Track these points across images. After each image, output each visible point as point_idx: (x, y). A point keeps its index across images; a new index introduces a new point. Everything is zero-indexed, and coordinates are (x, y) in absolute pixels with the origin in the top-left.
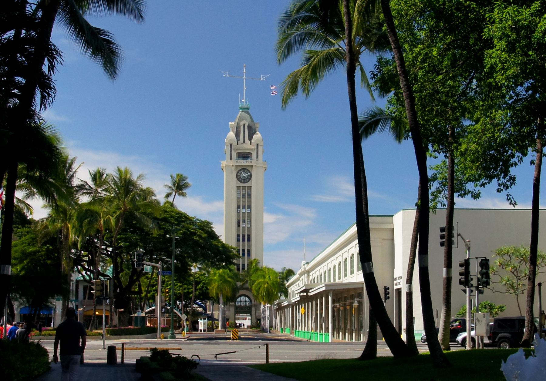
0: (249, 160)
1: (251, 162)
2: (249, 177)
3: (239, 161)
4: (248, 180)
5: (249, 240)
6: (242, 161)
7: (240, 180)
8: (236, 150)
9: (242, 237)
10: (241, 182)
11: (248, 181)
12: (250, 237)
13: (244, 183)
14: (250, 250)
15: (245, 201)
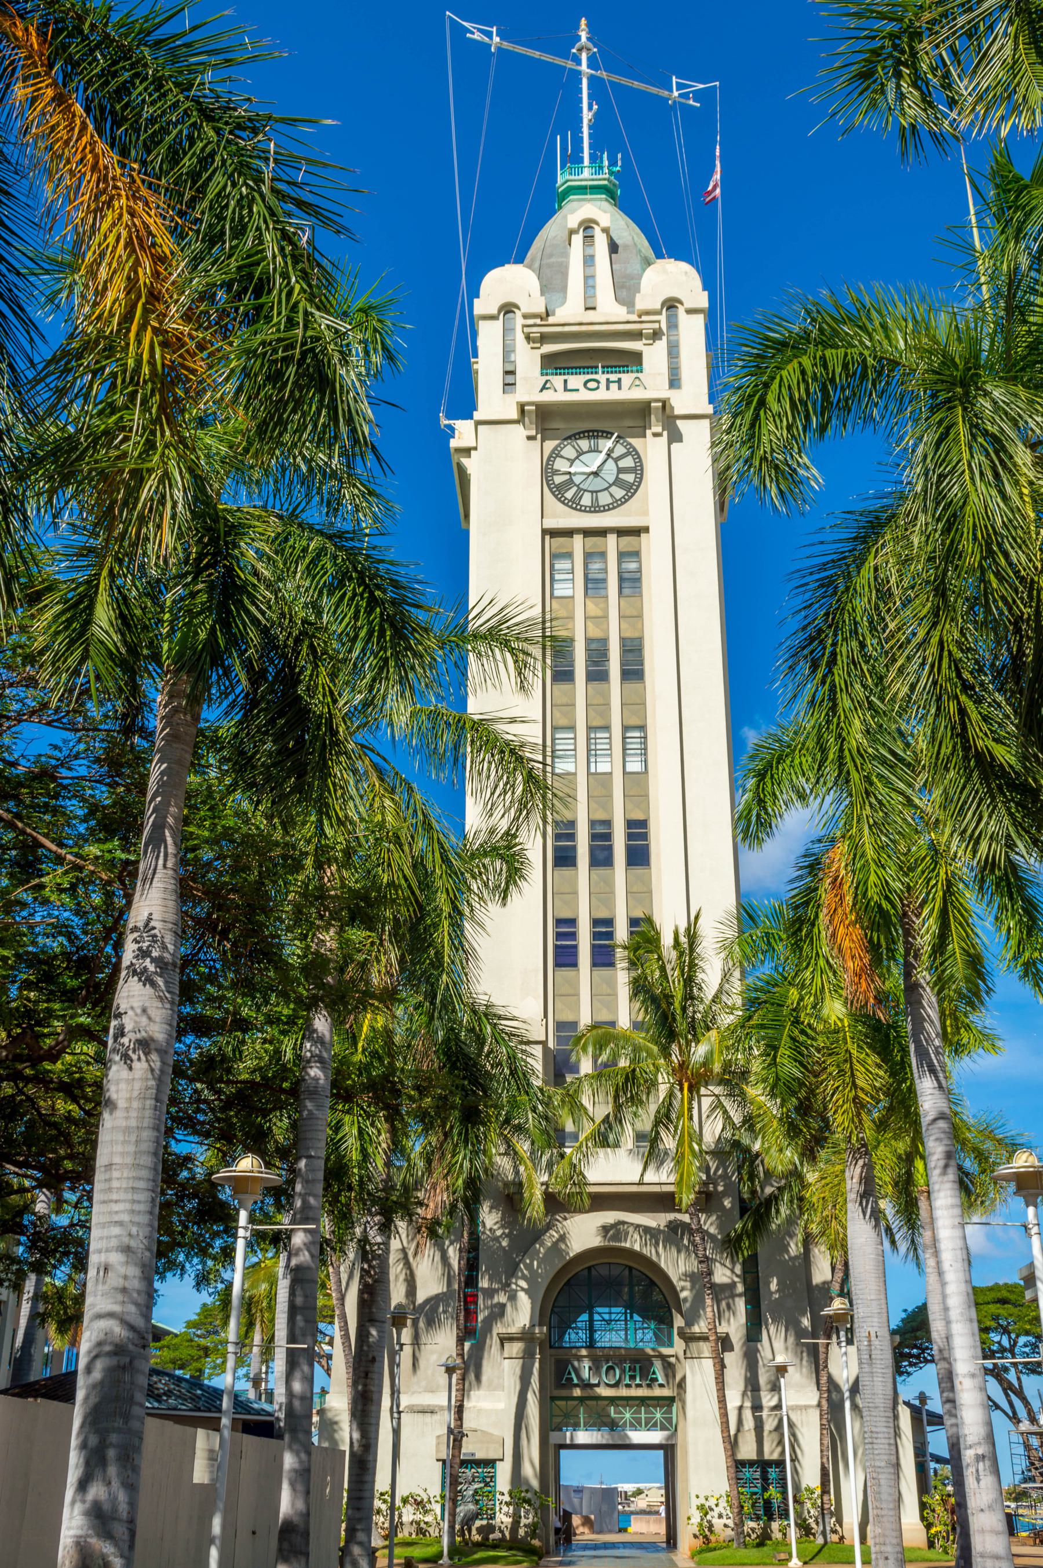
0: (627, 379)
1: (638, 383)
2: (630, 478)
3: (558, 381)
4: (620, 493)
5: (633, 672)
6: (576, 381)
7: (569, 495)
8: (544, 339)
9: (594, 837)
10: (574, 504)
11: (624, 500)
12: (645, 836)
13: (596, 509)
14: (643, 824)
15: (606, 617)
